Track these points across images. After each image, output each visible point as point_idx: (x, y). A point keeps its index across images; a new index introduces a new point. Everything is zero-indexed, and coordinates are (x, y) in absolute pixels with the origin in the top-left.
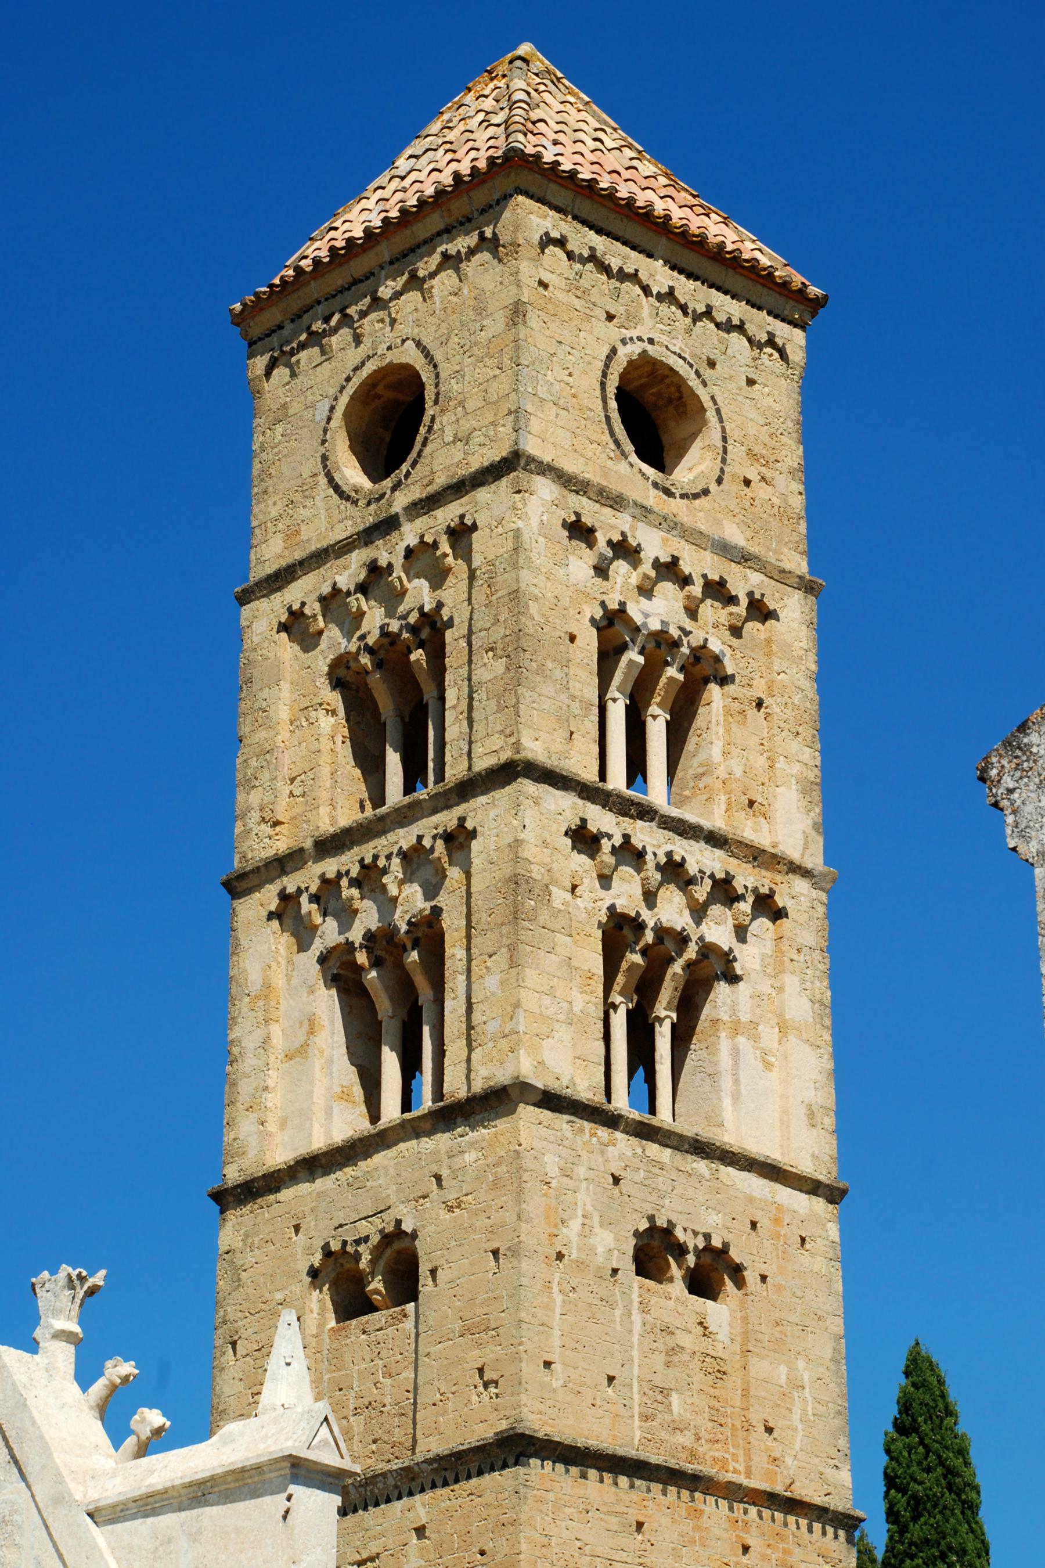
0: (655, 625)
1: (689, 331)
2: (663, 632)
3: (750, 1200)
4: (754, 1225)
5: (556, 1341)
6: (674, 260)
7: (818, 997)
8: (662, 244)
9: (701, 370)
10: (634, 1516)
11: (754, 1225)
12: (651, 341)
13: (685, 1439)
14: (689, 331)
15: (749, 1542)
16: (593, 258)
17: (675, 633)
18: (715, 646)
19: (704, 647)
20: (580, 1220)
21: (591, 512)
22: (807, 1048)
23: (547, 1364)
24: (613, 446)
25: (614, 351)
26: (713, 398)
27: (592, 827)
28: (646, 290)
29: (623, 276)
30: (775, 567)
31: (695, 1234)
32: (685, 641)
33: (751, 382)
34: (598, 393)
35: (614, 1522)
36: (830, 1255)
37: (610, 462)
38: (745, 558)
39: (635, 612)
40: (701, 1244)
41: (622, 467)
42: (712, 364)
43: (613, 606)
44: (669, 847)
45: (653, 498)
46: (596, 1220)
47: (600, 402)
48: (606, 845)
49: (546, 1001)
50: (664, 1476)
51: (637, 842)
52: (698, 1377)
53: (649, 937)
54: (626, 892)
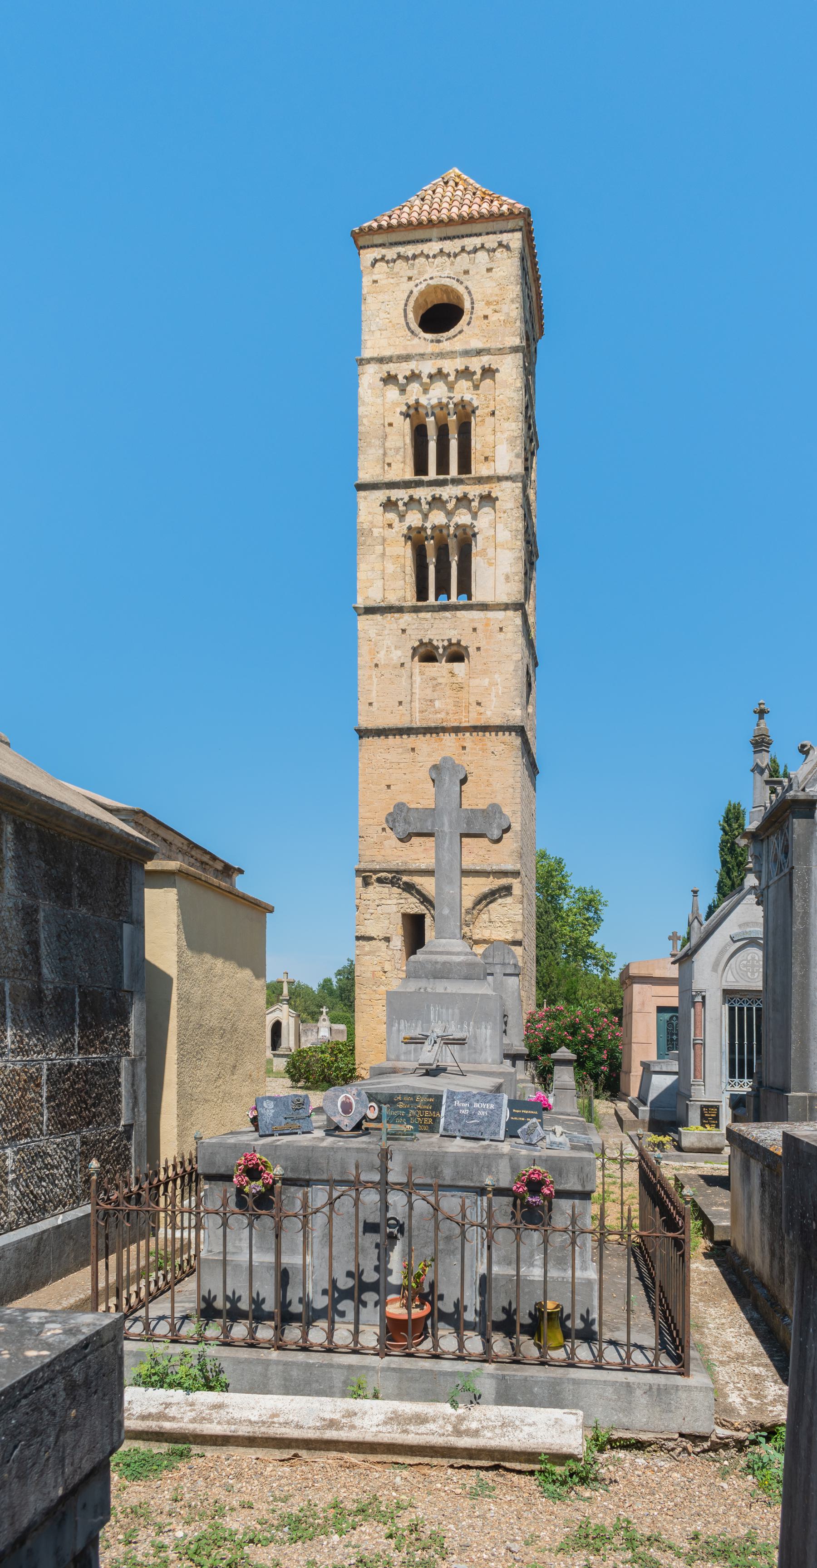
0: (434, 401)
1: (452, 264)
2: (440, 403)
3: (472, 620)
4: (475, 630)
5: (374, 694)
6: (443, 235)
7: (514, 528)
8: (435, 232)
9: (460, 278)
10: (410, 746)
11: (475, 630)
12: (431, 278)
13: (442, 715)
14: (452, 264)
15: (465, 745)
16: (399, 256)
17: (445, 401)
18: (467, 398)
19: (462, 400)
20: (385, 649)
21: (392, 368)
22: (507, 551)
23: (371, 704)
24: (410, 334)
25: (411, 292)
26: (467, 288)
27: (393, 499)
28: (427, 257)
29: (415, 257)
30: (495, 349)
31: (443, 640)
32: (451, 402)
33: (489, 270)
34: (403, 314)
35: (400, 750)
36: (516, 630)
37: (408, 343)
38: (479, 352)
39: (423, 401)
40: (446, 643)
41: (416, 341)
42: (466, 272)
43: (412, 402)
44: (433, 493)
45: (430, 348)
46: (393, 648)
47: (403, 319)
48: (400, 503)
49: (370, 573)
50: (423, 731)
51: (416, 497)
52: (448, 692)
53: (429, 532)
54: (414, 519)
